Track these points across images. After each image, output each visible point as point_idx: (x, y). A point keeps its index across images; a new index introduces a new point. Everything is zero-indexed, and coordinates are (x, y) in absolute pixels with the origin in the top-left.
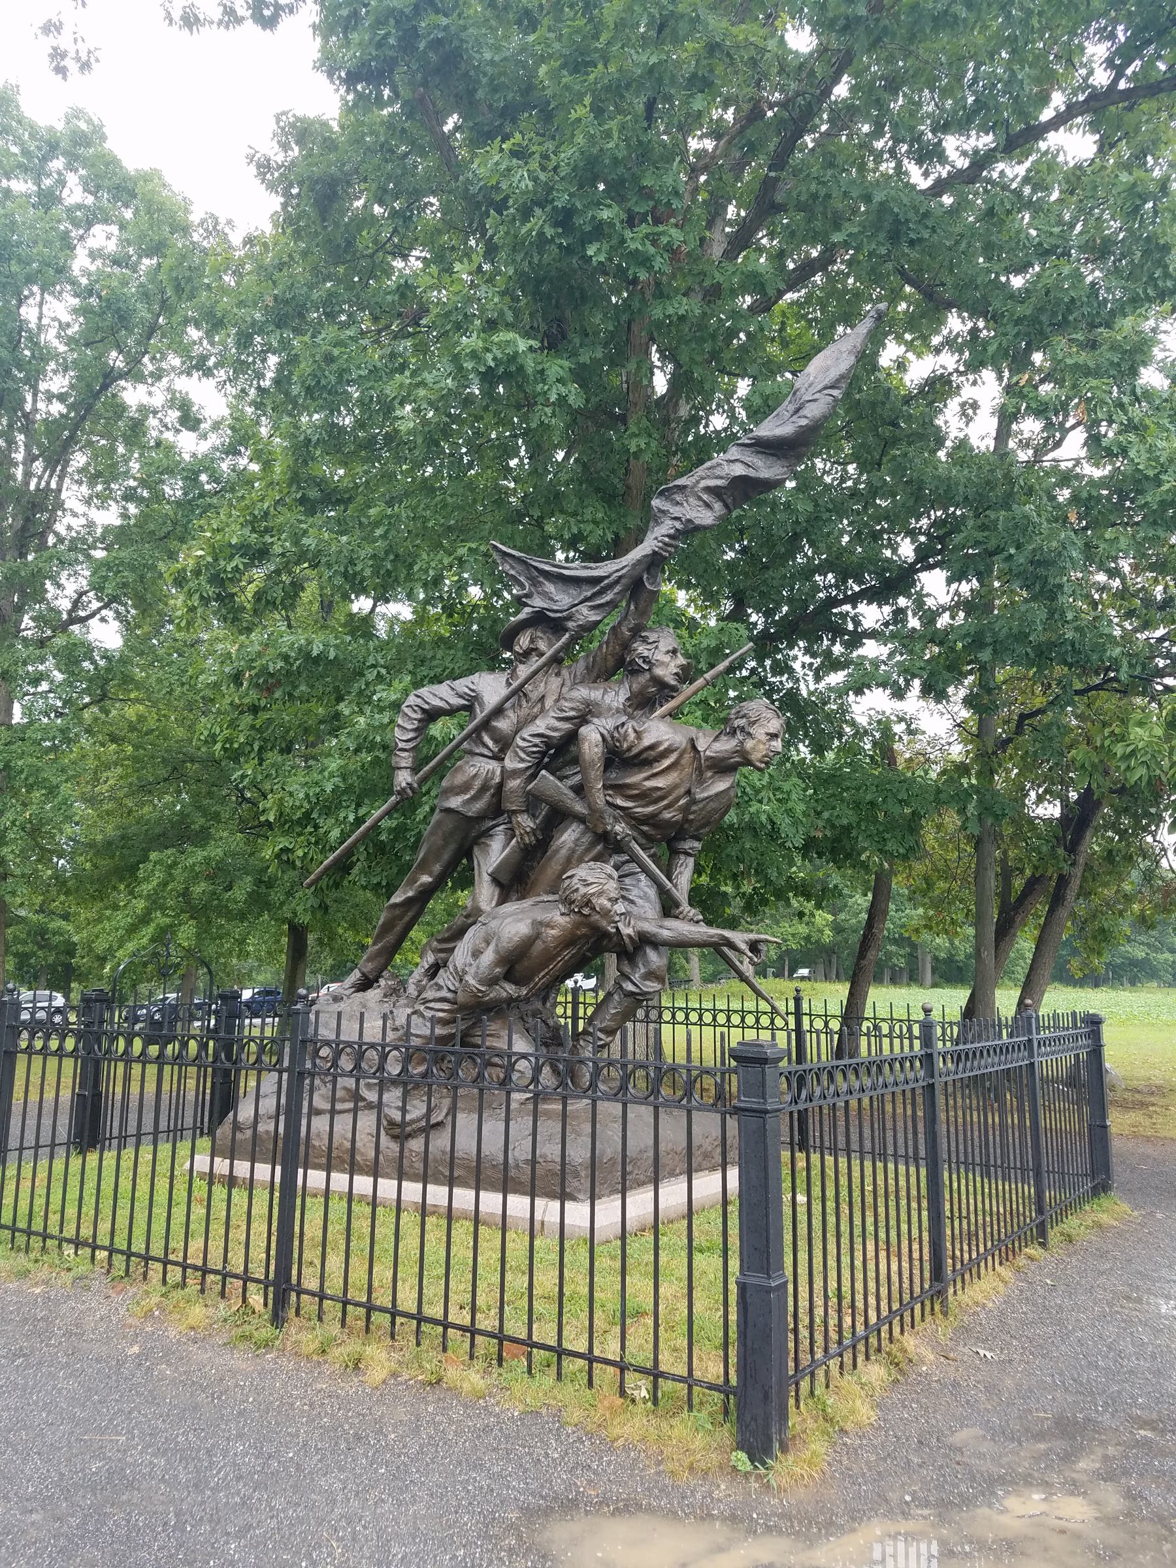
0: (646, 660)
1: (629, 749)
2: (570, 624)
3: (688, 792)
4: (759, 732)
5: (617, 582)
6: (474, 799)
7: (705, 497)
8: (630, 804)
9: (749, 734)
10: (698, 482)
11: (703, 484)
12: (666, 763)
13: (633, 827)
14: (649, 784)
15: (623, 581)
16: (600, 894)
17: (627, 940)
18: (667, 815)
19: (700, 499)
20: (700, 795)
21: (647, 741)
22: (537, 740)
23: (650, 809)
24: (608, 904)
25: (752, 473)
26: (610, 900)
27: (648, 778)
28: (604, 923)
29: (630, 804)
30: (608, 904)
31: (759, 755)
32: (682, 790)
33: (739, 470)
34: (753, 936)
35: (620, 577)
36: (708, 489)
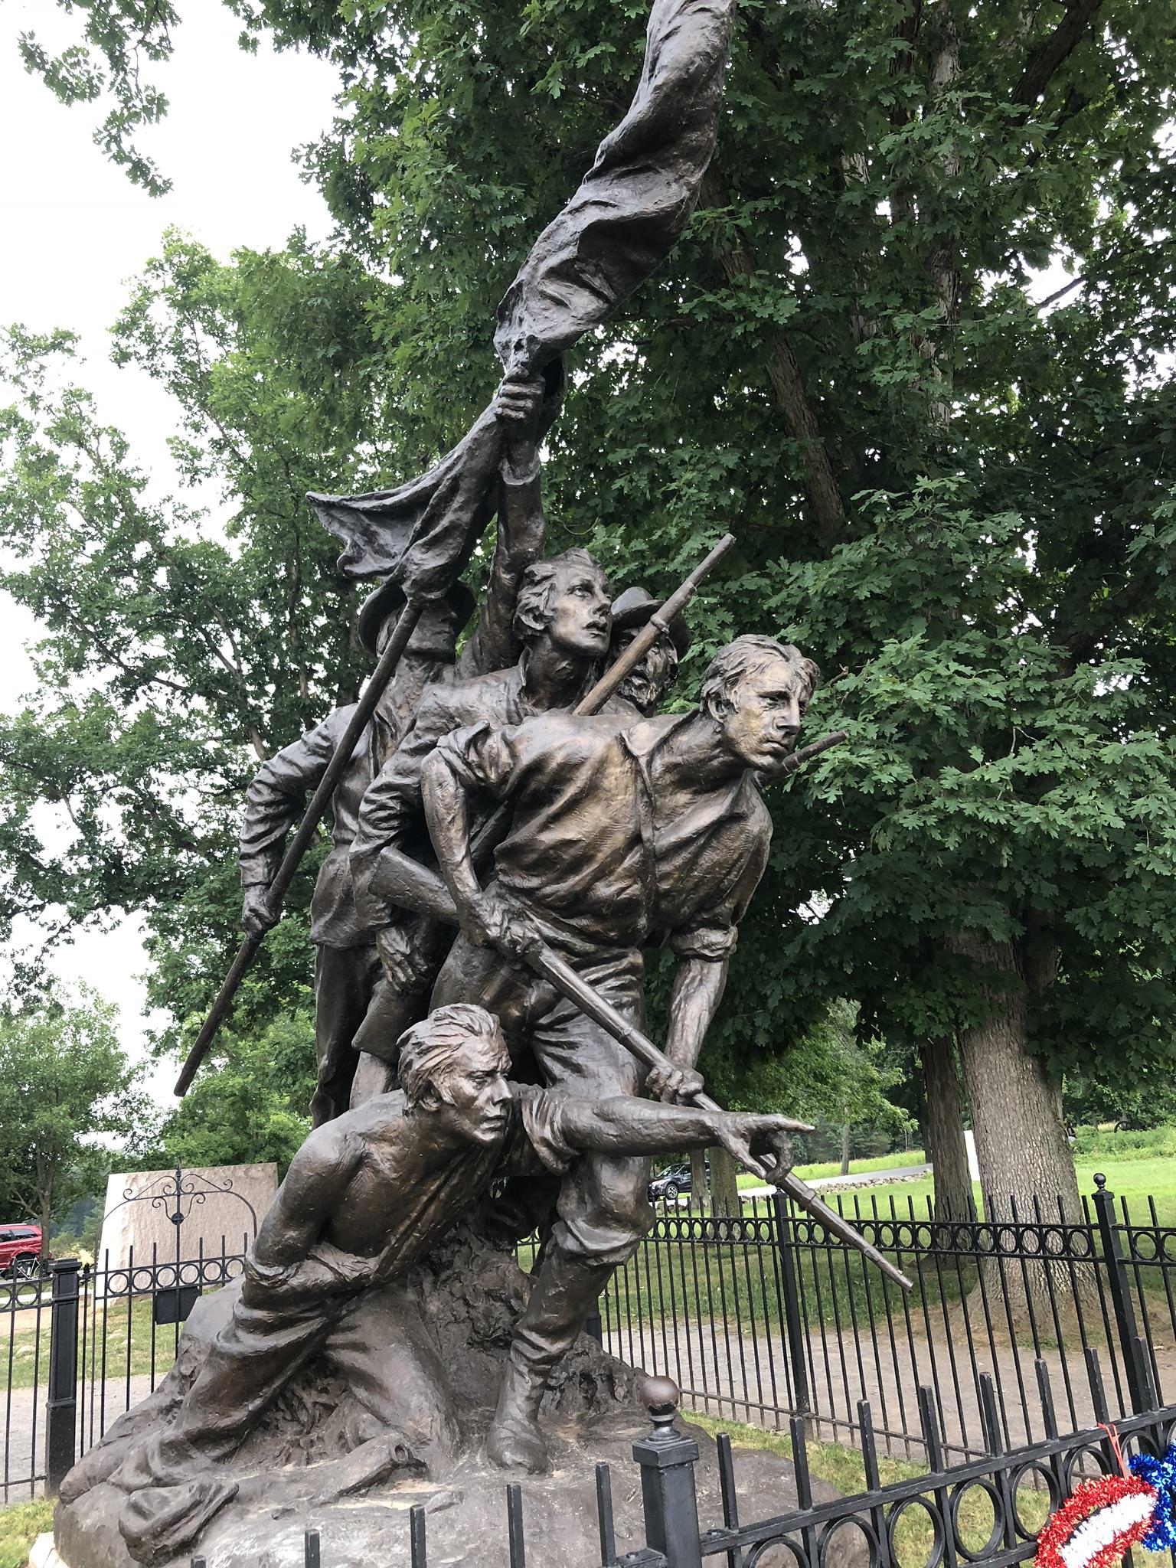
0: (533, 611)
1: (503, 779)
2: (405, 587)
3: (636, 840)
4: (744, 696)
5: (453, 489)
6: (339, 917)
7: (553, 288)
8: (534, 882)
9: (729, 704)
10: (535, 269)
11: (543, 268)
12: (571, 791)
13: (557, 924)
14: (549, 837)
15: (464, 484)
16: (450, 1067)
17: (544, 1151)
18: (604, 890)
19: (544, 295)
20: (667, 838)
21: (526, 759)
22: (383, 798)
23: (563, 887)
24: (468, 1087)
25: (610, 214)
26: (470, 1076)
27: (544, 827)
28: (466, 1124)
29: (534, 882)
30: (468, 1087)
31: (753, 742)
32: (619, 839)
33: (593, 215)
34: (753, 1119)
35: (456, 479)
36: (554, 273)
